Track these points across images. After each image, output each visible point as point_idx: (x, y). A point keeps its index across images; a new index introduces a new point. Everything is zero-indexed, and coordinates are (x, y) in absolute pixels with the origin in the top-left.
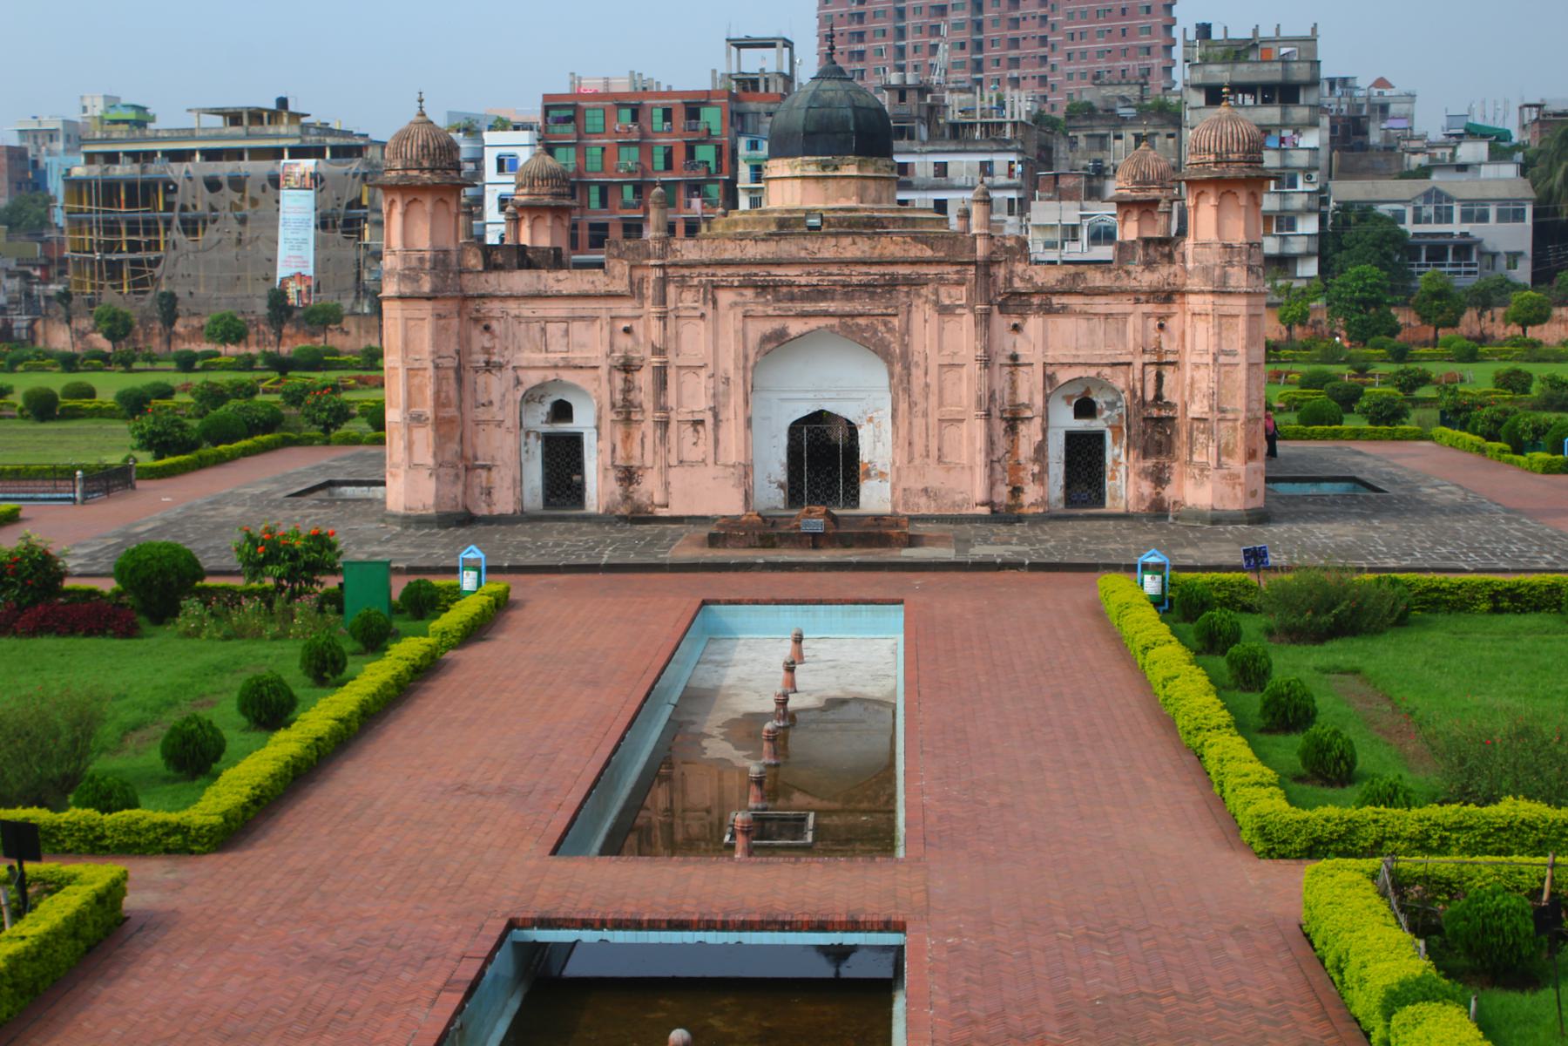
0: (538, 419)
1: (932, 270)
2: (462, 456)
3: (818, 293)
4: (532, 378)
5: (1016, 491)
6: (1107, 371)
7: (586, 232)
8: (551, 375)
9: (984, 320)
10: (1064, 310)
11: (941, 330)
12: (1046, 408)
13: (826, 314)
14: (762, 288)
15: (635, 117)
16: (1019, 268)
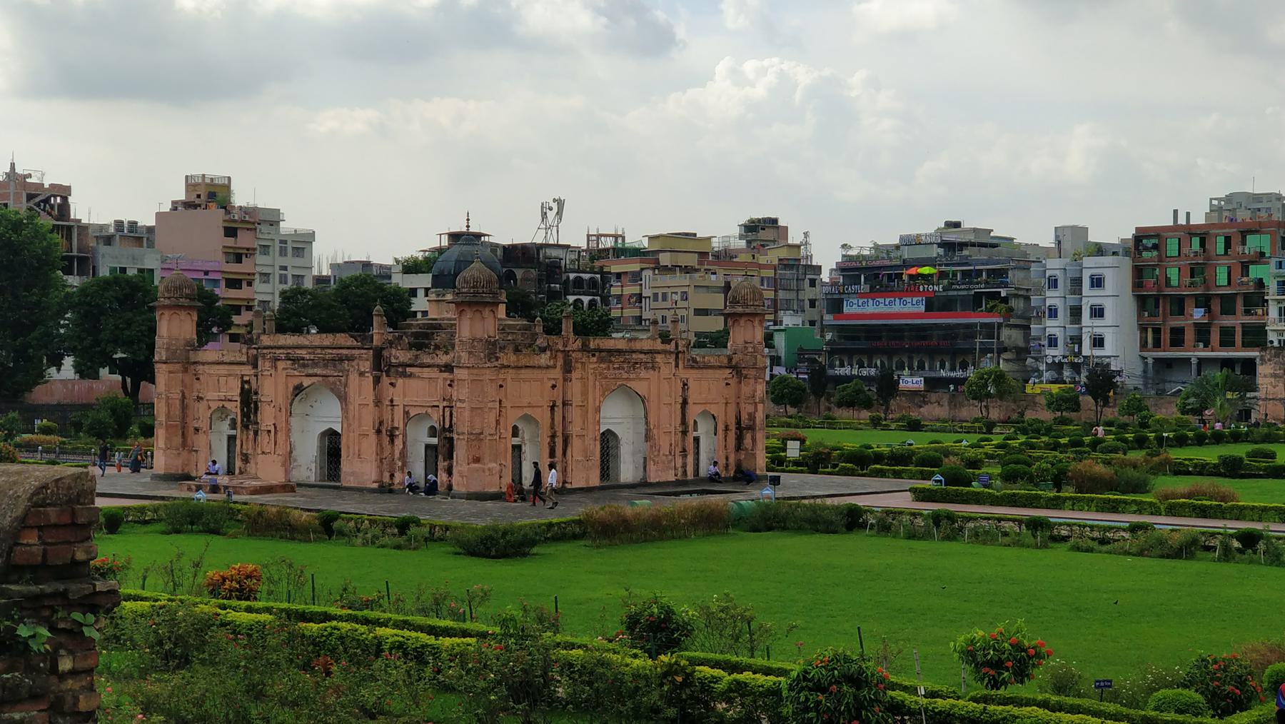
0: (225, 429)
1: (356, 352)
2: (184, 445)
3: (315, 364)
4: (214, 406)
5: (392, 476)
6: (430, 410)
7: (1168, 336)
8: (221, 404)
9: (377, 381)
10: (411, 375)
11: (360, 385)
12: (405, 429)
13: (316, 375)
14: (295, 360)
15: (1202, 244)
16: (394, 351)
